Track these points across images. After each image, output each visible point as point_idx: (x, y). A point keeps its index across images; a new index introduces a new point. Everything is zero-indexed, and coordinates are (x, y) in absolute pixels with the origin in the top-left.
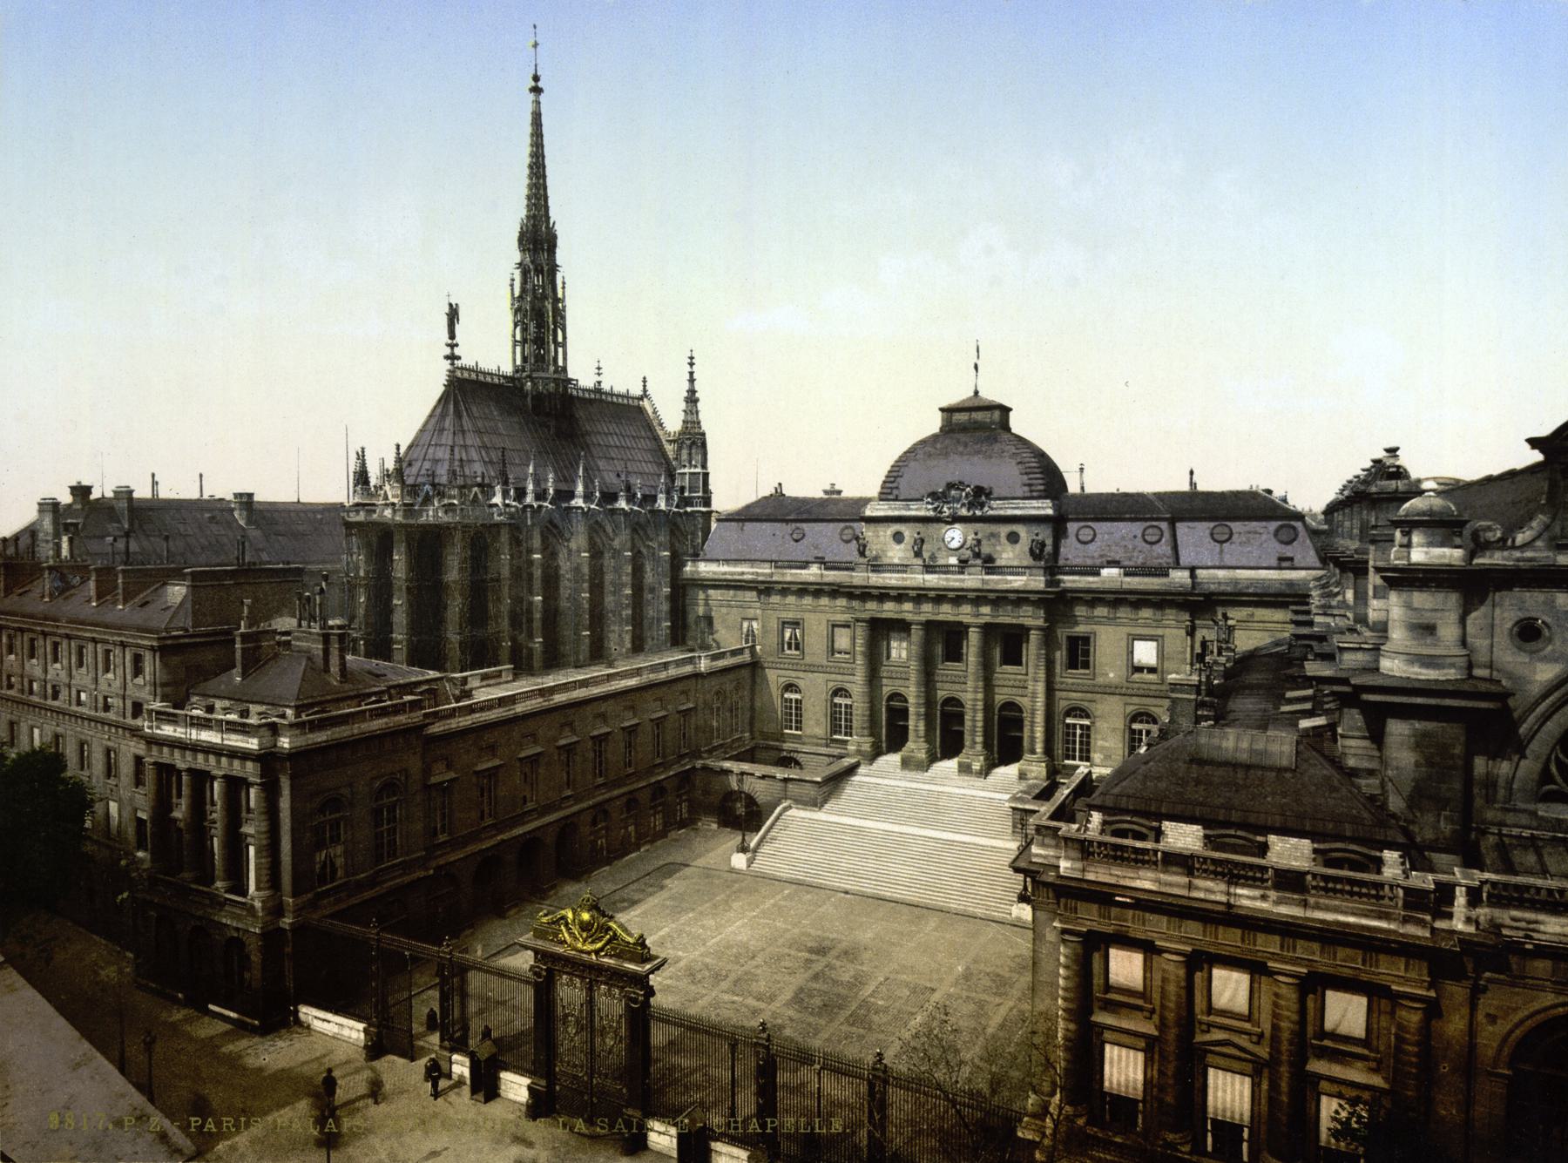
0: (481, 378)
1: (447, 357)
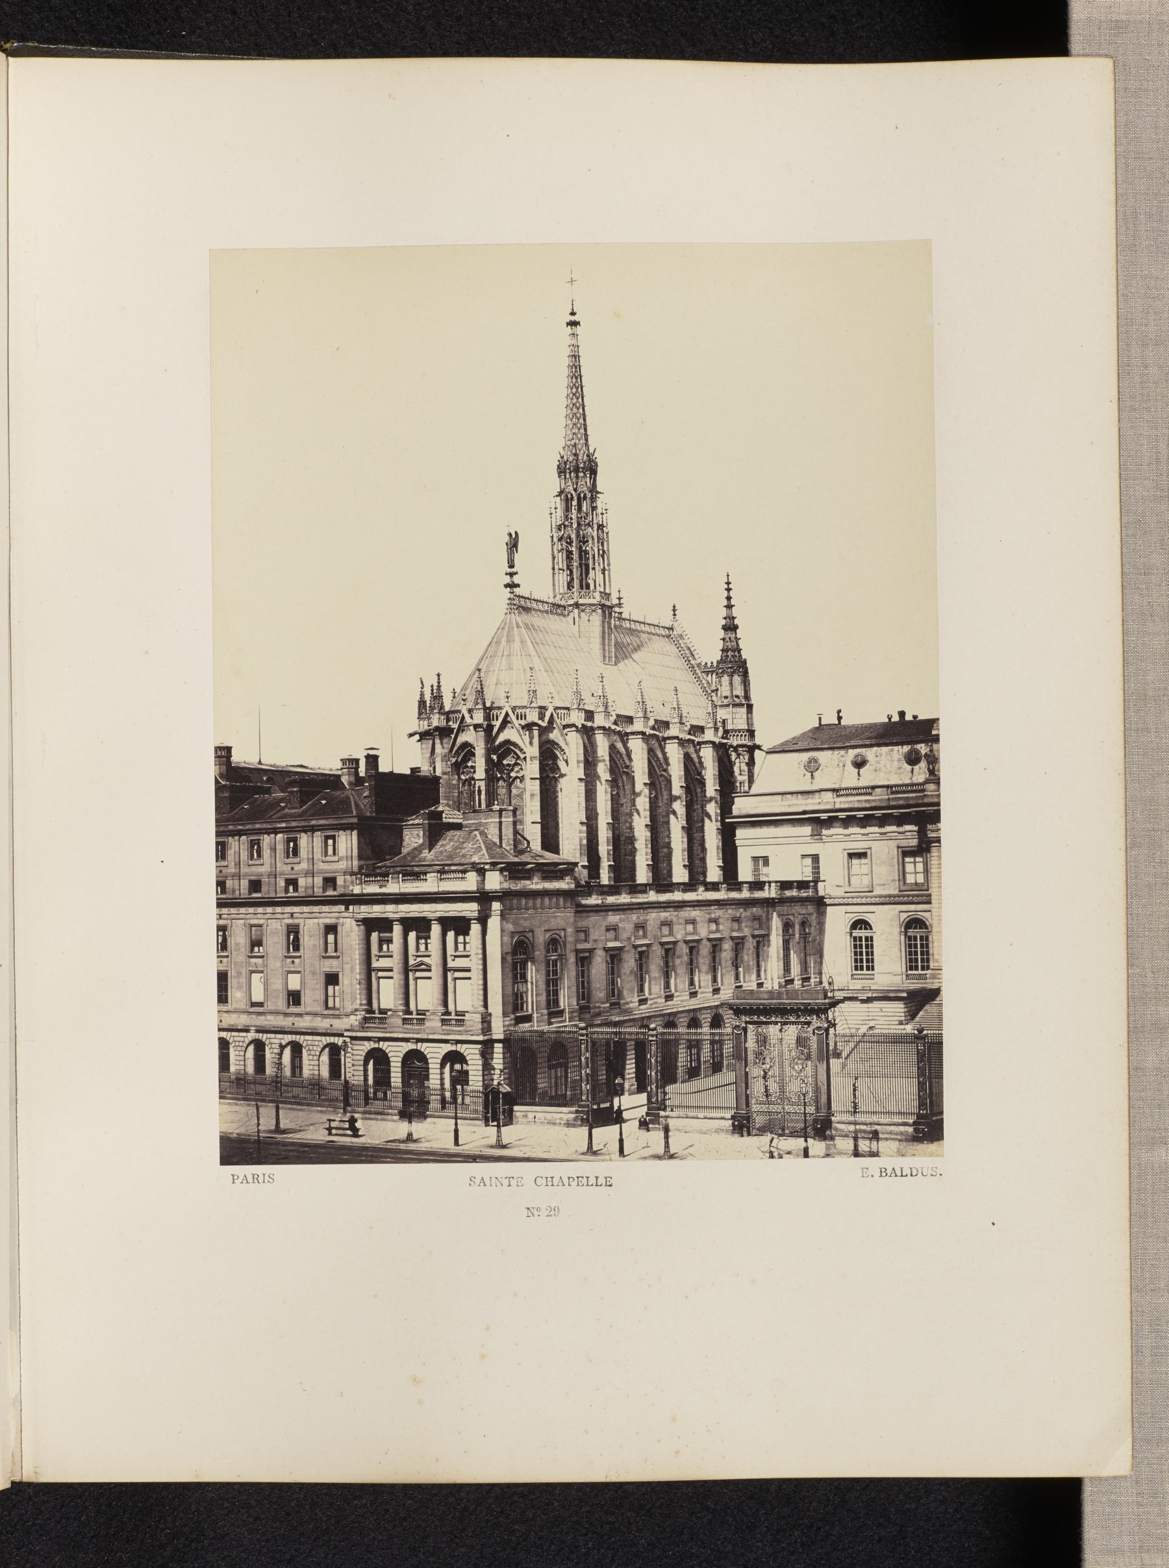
1: (507, 586)
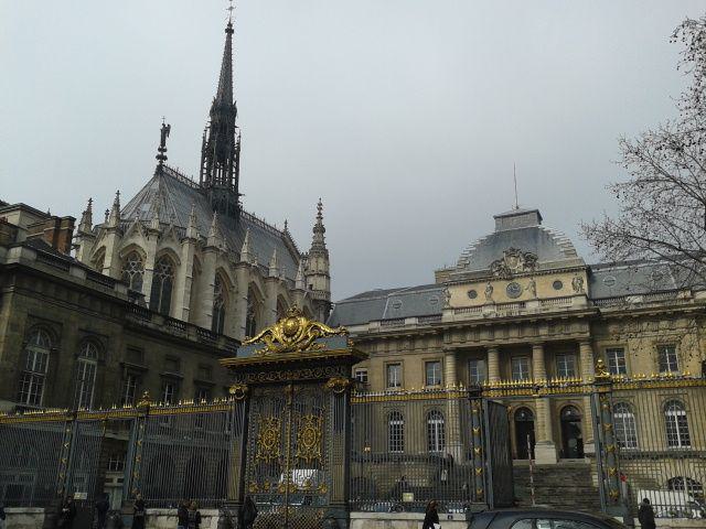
0: (179, 177)
